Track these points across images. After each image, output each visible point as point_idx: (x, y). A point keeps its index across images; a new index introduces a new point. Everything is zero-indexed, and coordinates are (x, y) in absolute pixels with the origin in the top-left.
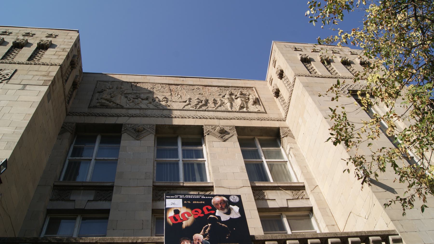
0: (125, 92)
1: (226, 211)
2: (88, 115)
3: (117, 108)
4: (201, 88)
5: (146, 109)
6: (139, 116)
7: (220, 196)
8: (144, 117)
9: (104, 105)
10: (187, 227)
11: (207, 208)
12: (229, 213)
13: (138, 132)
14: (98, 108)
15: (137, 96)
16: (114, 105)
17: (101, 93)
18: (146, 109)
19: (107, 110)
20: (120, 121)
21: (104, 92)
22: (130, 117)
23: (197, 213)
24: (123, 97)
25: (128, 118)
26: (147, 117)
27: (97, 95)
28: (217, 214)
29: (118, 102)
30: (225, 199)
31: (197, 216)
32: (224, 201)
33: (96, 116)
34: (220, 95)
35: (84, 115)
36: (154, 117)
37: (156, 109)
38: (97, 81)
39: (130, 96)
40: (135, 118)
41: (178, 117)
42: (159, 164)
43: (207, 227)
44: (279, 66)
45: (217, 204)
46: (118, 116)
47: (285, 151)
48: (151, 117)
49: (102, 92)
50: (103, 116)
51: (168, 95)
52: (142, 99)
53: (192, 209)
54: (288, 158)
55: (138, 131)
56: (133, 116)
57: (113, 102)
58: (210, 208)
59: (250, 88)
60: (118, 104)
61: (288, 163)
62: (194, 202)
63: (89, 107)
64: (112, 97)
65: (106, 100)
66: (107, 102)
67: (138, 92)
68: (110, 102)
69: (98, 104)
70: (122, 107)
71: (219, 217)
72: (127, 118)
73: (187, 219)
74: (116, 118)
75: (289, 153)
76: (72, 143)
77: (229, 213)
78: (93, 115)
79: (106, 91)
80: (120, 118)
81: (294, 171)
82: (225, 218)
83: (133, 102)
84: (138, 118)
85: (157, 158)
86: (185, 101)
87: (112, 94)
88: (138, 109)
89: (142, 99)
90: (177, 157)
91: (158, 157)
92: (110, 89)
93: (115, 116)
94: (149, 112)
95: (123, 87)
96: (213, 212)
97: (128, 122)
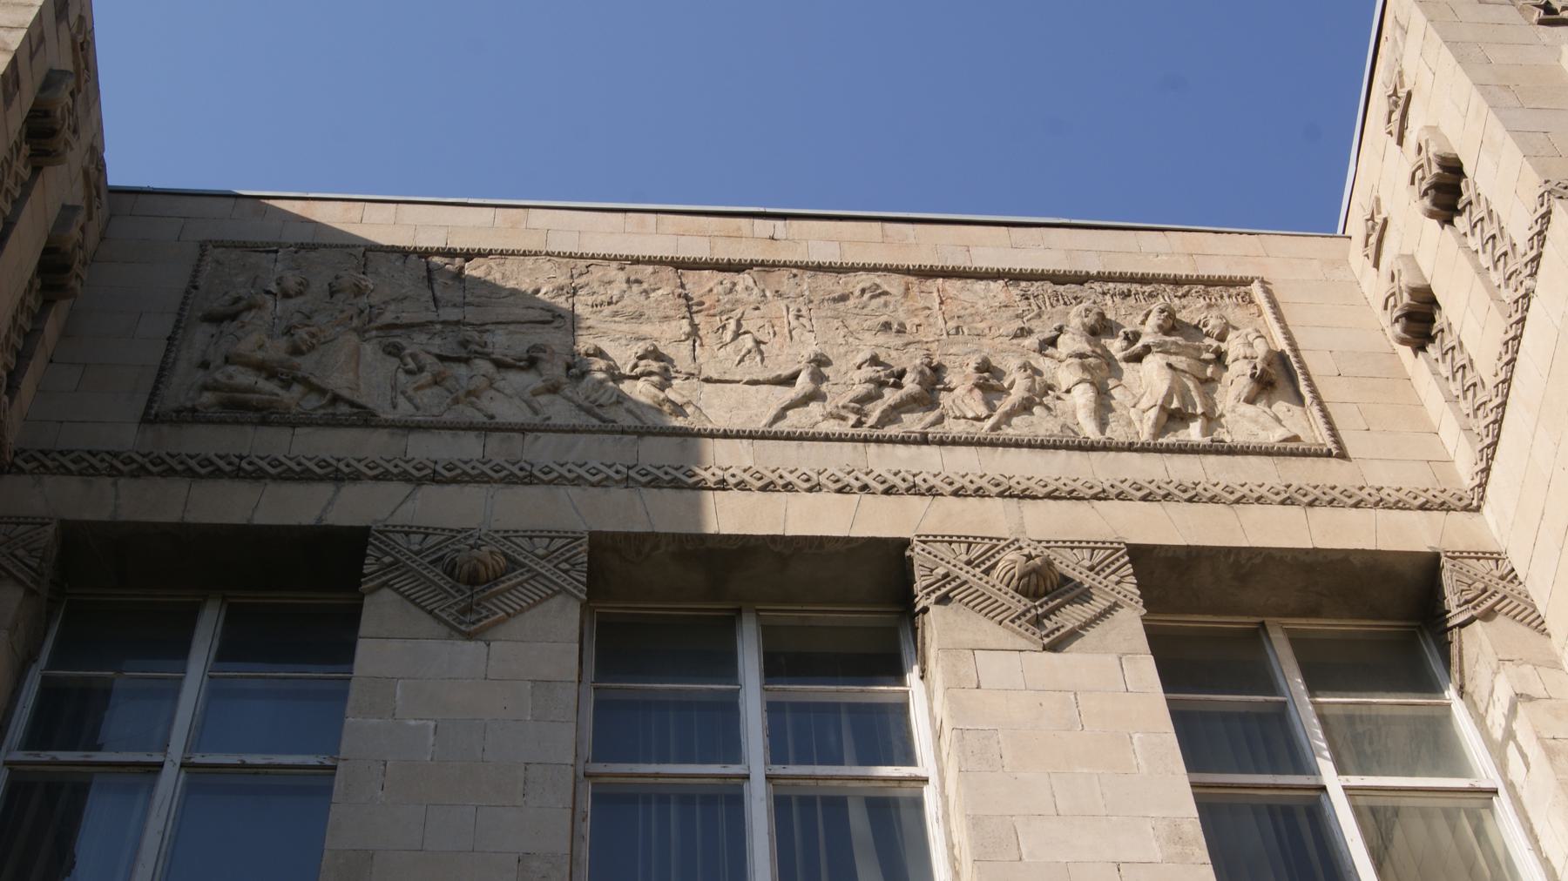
0: (388, 317)
2: (141, 472)
3: (334, 423)
4: (894, 284)
5: (523, 430)
6: (481, 479)
8: (511, 480)
9: (244, 406)
13: (470, 587)
14: (210, 422)
15: (464, 344)
16: (313, 401)
17: (228, 327)
18: (523, 430)
19: (267, 433)
20: (350, 507)
21: (247, 317)
22: (419, 482)
24: (370, 350)
25: (405, 488)
26: (530, 480)
27: (201, 335)
29: (338, 381)
33: (191, 473)
34: (1024, 333)
35: (114, 472)
36: (577, 481)
37: (589, 431)
38: (203, 246)
39: (416, 344)
40: (453, 488)
41: (741, 486)
42: (613, 807)
44: (1433, 130)
46: (337, 475)
47: (1480, 720)
48: (561, 481)
49: (233, 317)
50: (238, 474)
51: (669, 334)
52: (500, 365)
54: (1502, 767)
55: (473, 580)
56: (435, 479)
57: (305, 381)
59: (1229, 283)
60: (336, 399)
61: (1502, 803)
63: (149, 419)
64: (296, 351)
65: (266, 369)
66: (263, 384)
67: (471, 315)
68: (287, 385)
69: (208, 397)
70: (365, 418)
72: (399, 489)
74: (325, 490)
75: (1510, 734)
76: (30, 658)
78: (170, 472)
79: (260, 307)
80: (350, 491)
81: (1545, 862)
83: (437, 381)
84: (471, 490)
85: (596, 759)
86: (786, 372)
87: (302, 333)
88: (471, 427)
89: (500, 365)
90: (732, 749)
91: (605, 748)
92: (286, 295)
93: (321, 479)
94: (542, 451)
95: (369, 282)
97: (403, 517)
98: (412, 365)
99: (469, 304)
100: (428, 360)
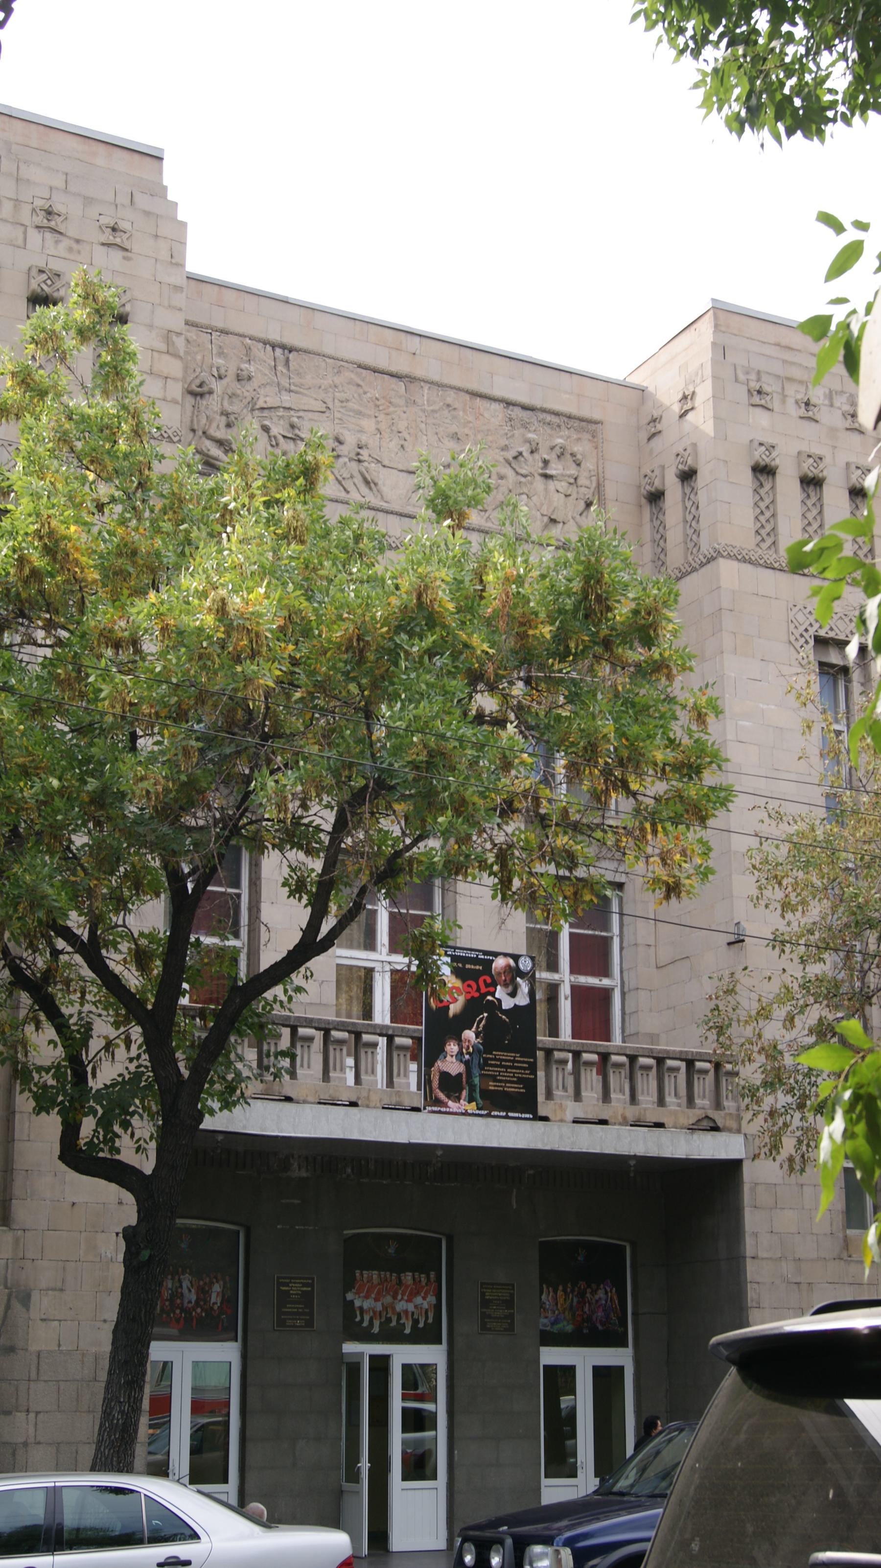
0: (261, 404)
1: (510, 988)
7: (506, 955)
10: (455, 1016)
11: (485, 981)
12: (513, 994)
15: (293, 426)
23: (470, 989)
24: (256, 426)
28: (497, 996)
30: (512, 962)
31: (469, 996)
32: (509, 966)
34: (505, 448)
43: (482, 1019)
45: (499, 974)
49: (202, 395)
53: (463, 981)
58: (489, 980)
62: (468, 966)
64: (229, 425)
65: (220, 443)
71: (499, 1001)
73: (455, 1000)
77: (513, 994)
82: (508, 1003)
87: (232, 417)
92: (220, 378)
96: (491, 989)
98: (274, 443)
99: (290, 391)
100: (281, 440)
